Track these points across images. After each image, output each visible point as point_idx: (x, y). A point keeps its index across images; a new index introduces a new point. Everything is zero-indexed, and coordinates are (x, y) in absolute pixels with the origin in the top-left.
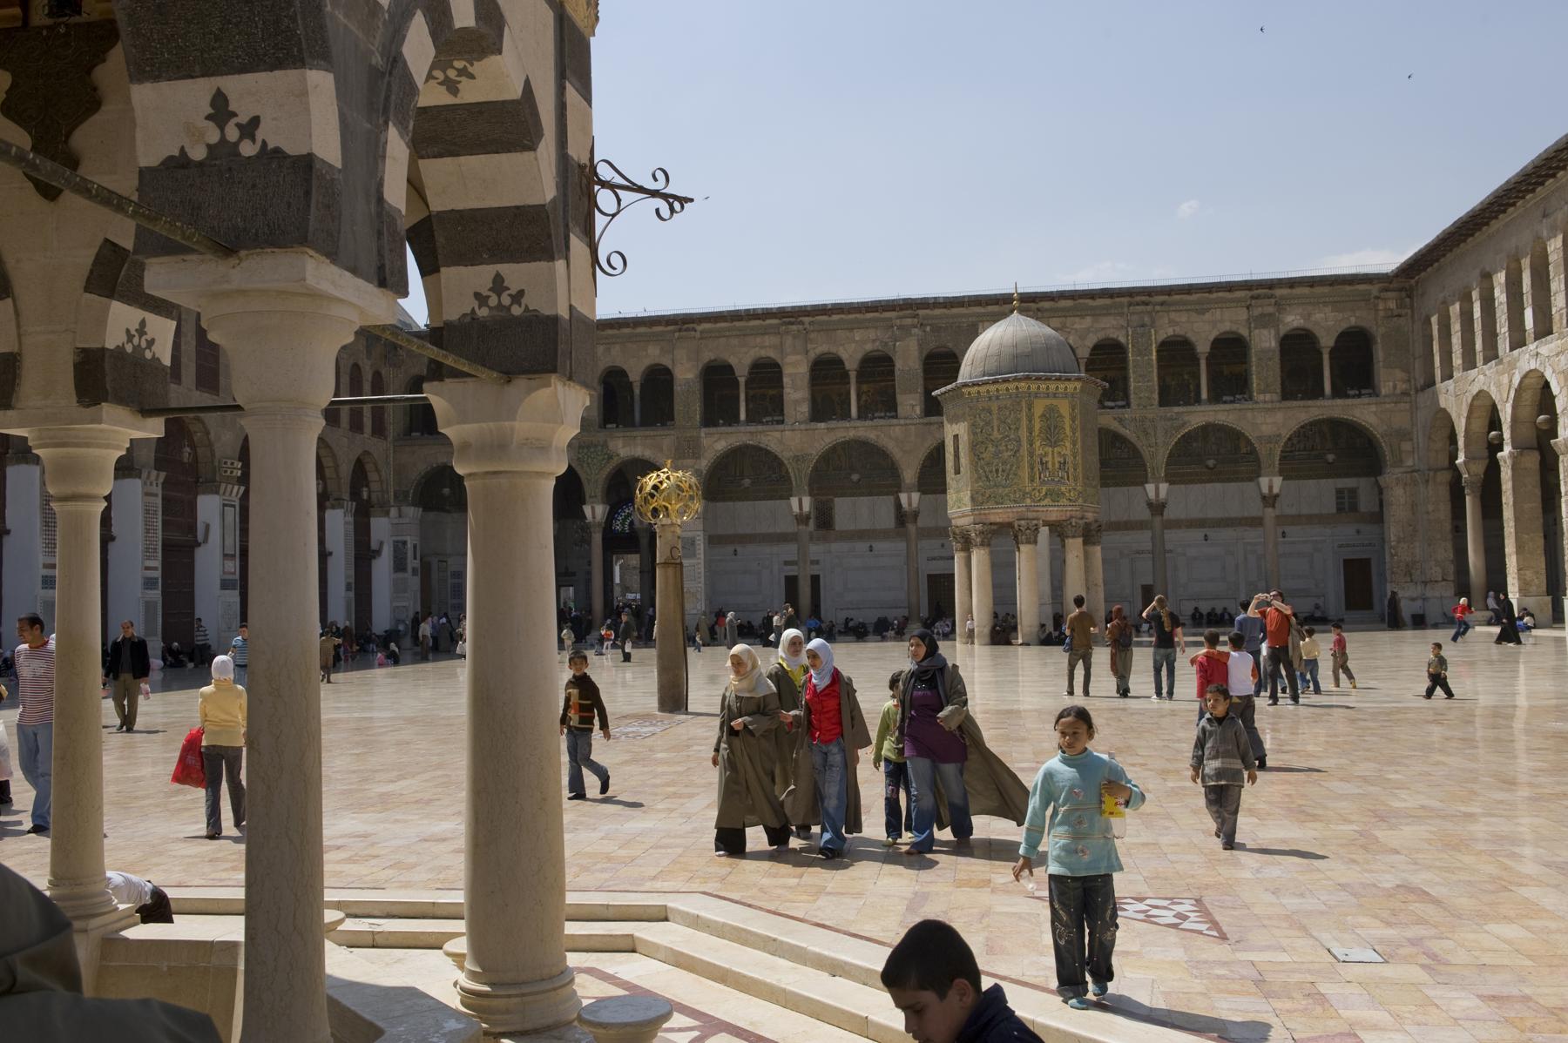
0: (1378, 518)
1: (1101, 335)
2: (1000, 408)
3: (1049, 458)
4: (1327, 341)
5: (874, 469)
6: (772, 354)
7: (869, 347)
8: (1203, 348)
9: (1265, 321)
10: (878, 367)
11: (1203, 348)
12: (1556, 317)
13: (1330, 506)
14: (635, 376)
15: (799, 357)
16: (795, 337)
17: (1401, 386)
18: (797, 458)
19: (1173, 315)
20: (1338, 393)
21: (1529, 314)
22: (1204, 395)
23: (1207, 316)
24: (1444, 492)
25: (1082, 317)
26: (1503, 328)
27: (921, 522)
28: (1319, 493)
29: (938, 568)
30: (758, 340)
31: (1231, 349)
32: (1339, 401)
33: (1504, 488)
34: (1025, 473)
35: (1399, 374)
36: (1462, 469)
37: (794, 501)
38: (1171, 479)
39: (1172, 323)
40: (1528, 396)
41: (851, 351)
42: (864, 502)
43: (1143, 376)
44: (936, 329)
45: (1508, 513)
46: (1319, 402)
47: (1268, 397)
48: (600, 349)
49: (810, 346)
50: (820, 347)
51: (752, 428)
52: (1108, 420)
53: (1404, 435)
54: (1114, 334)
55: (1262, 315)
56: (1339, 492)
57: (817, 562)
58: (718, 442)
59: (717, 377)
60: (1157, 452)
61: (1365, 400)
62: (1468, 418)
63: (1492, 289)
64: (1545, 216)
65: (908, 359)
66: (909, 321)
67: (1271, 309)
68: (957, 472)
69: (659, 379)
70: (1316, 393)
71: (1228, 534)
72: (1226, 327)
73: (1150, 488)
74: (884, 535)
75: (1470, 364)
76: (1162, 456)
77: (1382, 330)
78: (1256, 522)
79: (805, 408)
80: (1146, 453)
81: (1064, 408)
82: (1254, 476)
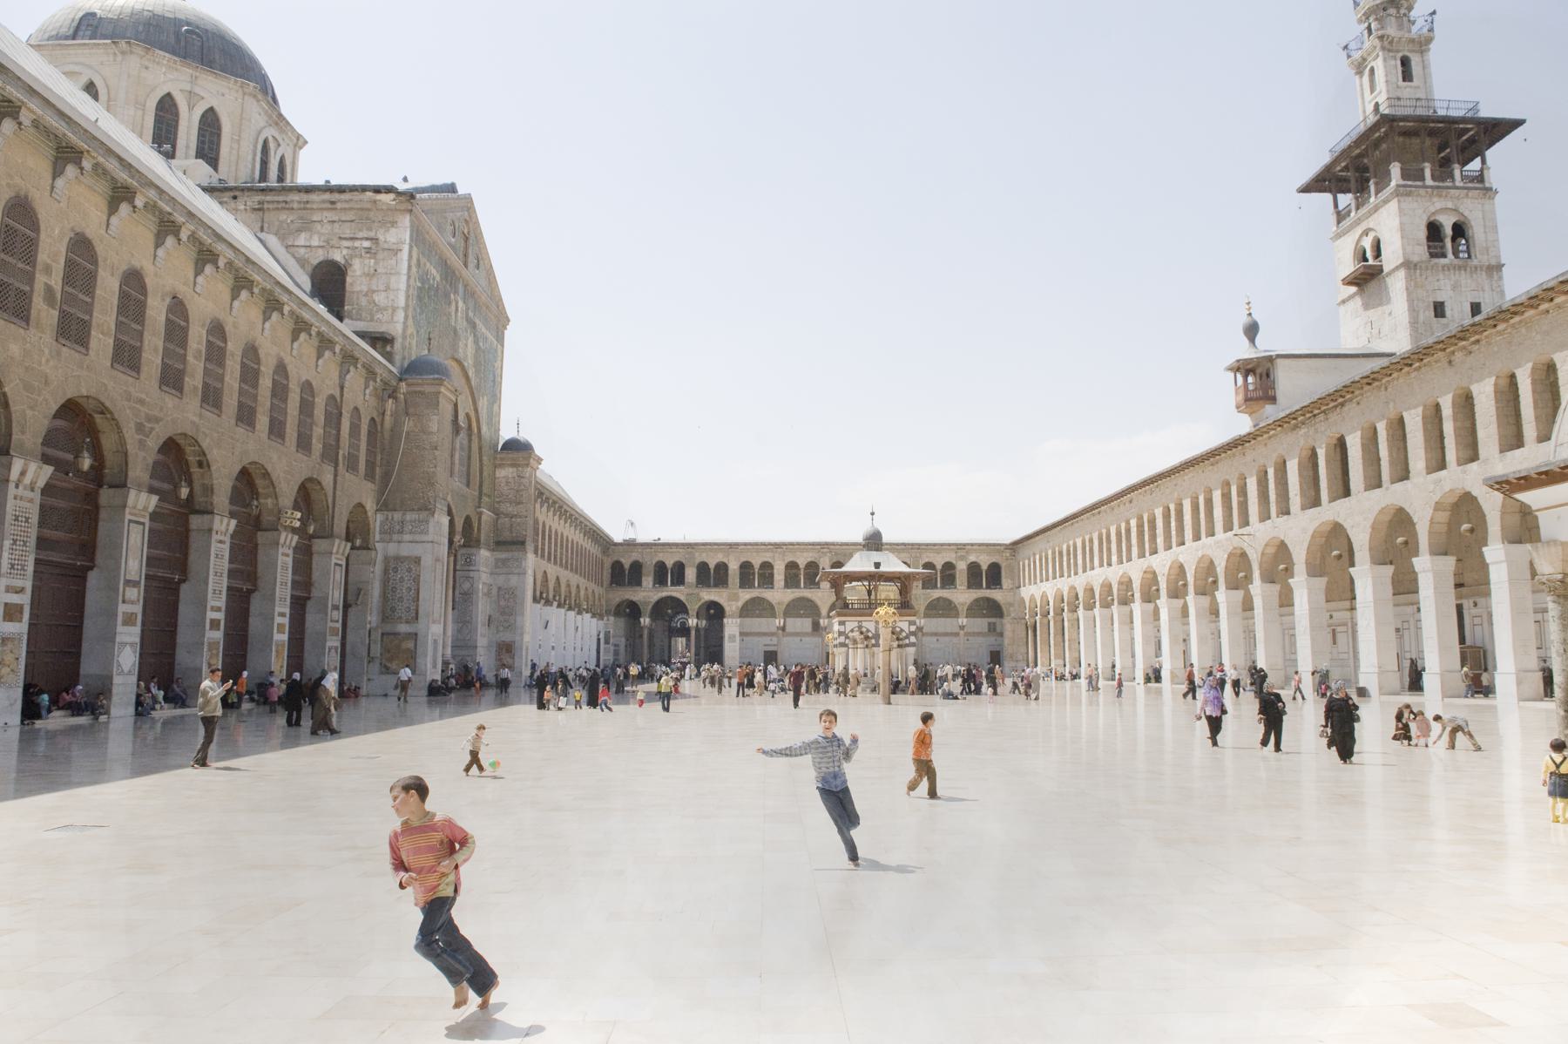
0: (1001, 635)
4: (984, 567)
9: (962, 558)
14: (712, 566)
20: (988, 587)
28: (981, 624)
38: (926, 616)
42: (799, 620)
50: (790, 558)
53: (1011, 605)
58: (746, 595)
59: (746, 567)
69: (722, 568)
70: (980, 587)
74: (806, 634)
76: (922, 609)
78: (957, 634)
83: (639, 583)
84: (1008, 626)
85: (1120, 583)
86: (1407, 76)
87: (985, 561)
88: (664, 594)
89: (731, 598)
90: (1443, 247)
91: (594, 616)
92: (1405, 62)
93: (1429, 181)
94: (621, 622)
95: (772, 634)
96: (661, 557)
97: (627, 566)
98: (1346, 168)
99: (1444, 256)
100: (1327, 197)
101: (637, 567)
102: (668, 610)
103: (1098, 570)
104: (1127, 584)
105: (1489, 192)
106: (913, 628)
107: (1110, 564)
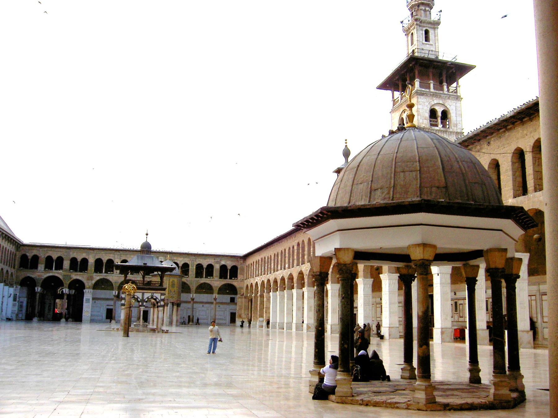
4: (229, 268)
8: (205, 266)
9: (217, 262)
11: (205, 266)
13: (229, 301)
14: (79, 260)
17: (242, 278)
31: (210, 267)
43: (192, 270)
48: (71, 253)
51: (106, 274)
56: (231, 298)
59: (99, 262)
60: (193, 287)
69: (85, 261)
70: (226, 278)
71: (207, 305)
72: (210, 263)
83: (36, 268)
84: (239, 300)
85: (289, 279)
86: (427, 39)
87: (229, 264)
88: (51, 274)
89: (89, 278)
90: (437, 122)
91: (6, 284)
92: (427, 32)
93: (432, 90)
94: (25, 290)
95: (112, 299)
96: (50, 253)
97: (30, 258)
98: (398, 80)
99: (437, 126)
100: (389, 92)
101: (36, 258)
102: (53, 284)
103: (280, 272)
104: (291, 278)
105: (458, 98)
106: (163, 297)
107: (285, 269)
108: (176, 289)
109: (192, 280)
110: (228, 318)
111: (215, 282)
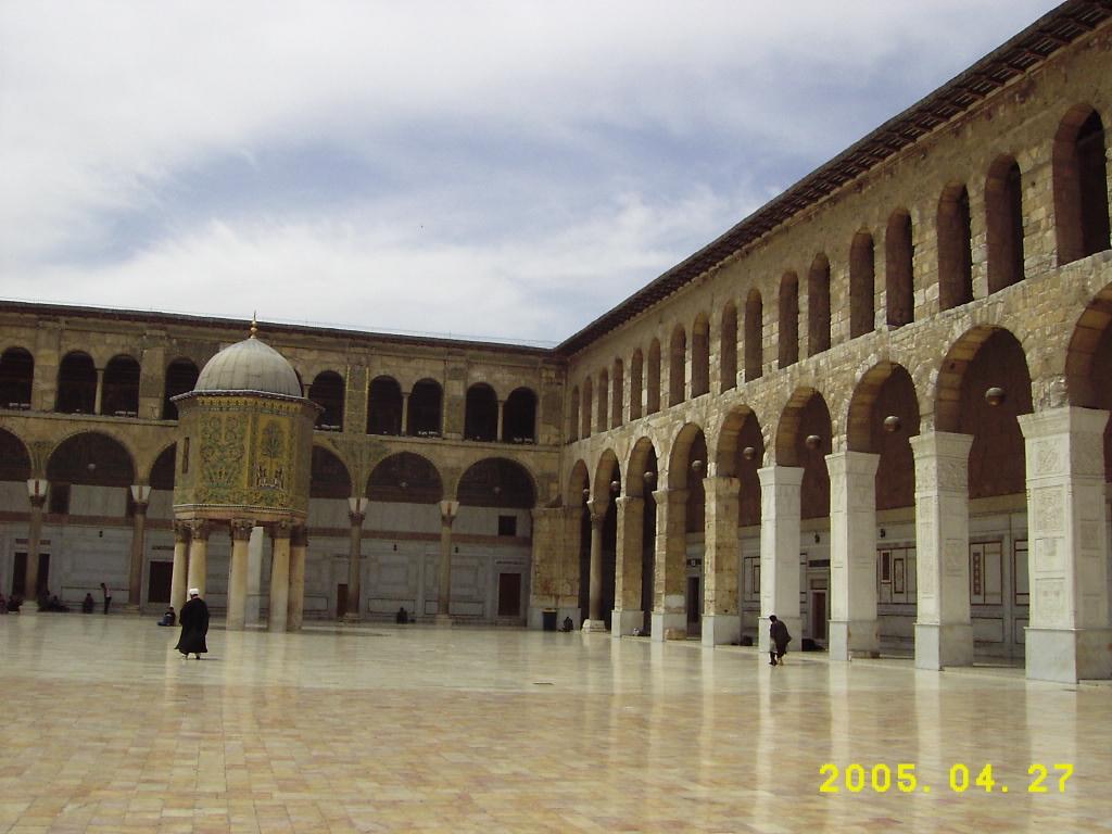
0: (528, 542)
1: (325, 368)
2: (229, 419)
3: (267, 467)
4: (503, 396)
5: (111, 463)
6: (26, 345)
7: (119, 351)
8: (407, 388)
9: (457, 374)
10: (124, 371)
11: (407, 388)
12: (662, 400)
13: (493, 528)
15: (52, 352)
16: (50, 332)
17: (554, 440)
18: (38, 444)
19: (385, 359)
20: (507, 439)
21: (645, 393)
22: (404, 429)
23: (413, 364)
24: (576, 524)
25: (310, 350)
26: (627, 403)
27: (149, 515)
28: (485, 519)
29: (161, 556)
30: (14, 331)
31: (429, 393)
32: (508, 446)
33: (618, 525)
34: (245, 478)
35: (553, 430)
36: (591, 508)
37: (31, 484)
38: (372, 495)
39: (384, 365)
40: (640, 456)
41: (102, 351)
42: (98, 492)
43: (356, 407)
44: (182, 344)
45: (619, 545)
46: (493, 445)
47: (454, 435)
49: (62, 343)
50: (73, 344)
52: (322, 438)
53: (552, 478)
54: (335, 368)
55: (456, 369)
56: (502, 520)
57: (49, 543)
60: (361, 471)
61: (527, 447)
62: (598, 469)
63: (622, 372)
64: (661, 322)
65: (153, 366)
66: (159, 333)
67: (461, 365)
68: (185, 471)
70: (491, 437)
71: (412, 546)
72: (427, 374)
73: (353, 502)
74: (114, 522)
75: (603, 427)
76: (365, 474)
77: (543, 393)
79: (51, 399)
80: (352, 470)
81: (285, 423)
82: (436, 500)
87: (504, 382)
108: (284, 460)
109: (355, 442)
110: (491, 595)
111: (446, 452)
